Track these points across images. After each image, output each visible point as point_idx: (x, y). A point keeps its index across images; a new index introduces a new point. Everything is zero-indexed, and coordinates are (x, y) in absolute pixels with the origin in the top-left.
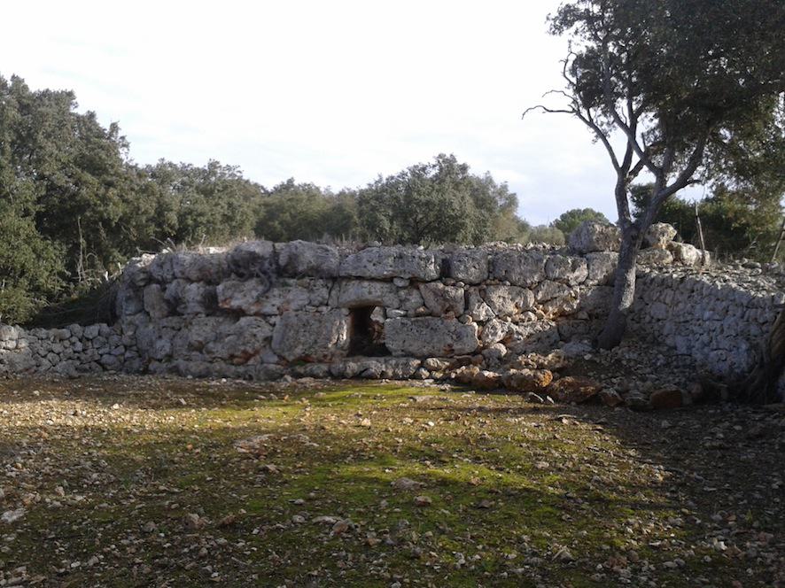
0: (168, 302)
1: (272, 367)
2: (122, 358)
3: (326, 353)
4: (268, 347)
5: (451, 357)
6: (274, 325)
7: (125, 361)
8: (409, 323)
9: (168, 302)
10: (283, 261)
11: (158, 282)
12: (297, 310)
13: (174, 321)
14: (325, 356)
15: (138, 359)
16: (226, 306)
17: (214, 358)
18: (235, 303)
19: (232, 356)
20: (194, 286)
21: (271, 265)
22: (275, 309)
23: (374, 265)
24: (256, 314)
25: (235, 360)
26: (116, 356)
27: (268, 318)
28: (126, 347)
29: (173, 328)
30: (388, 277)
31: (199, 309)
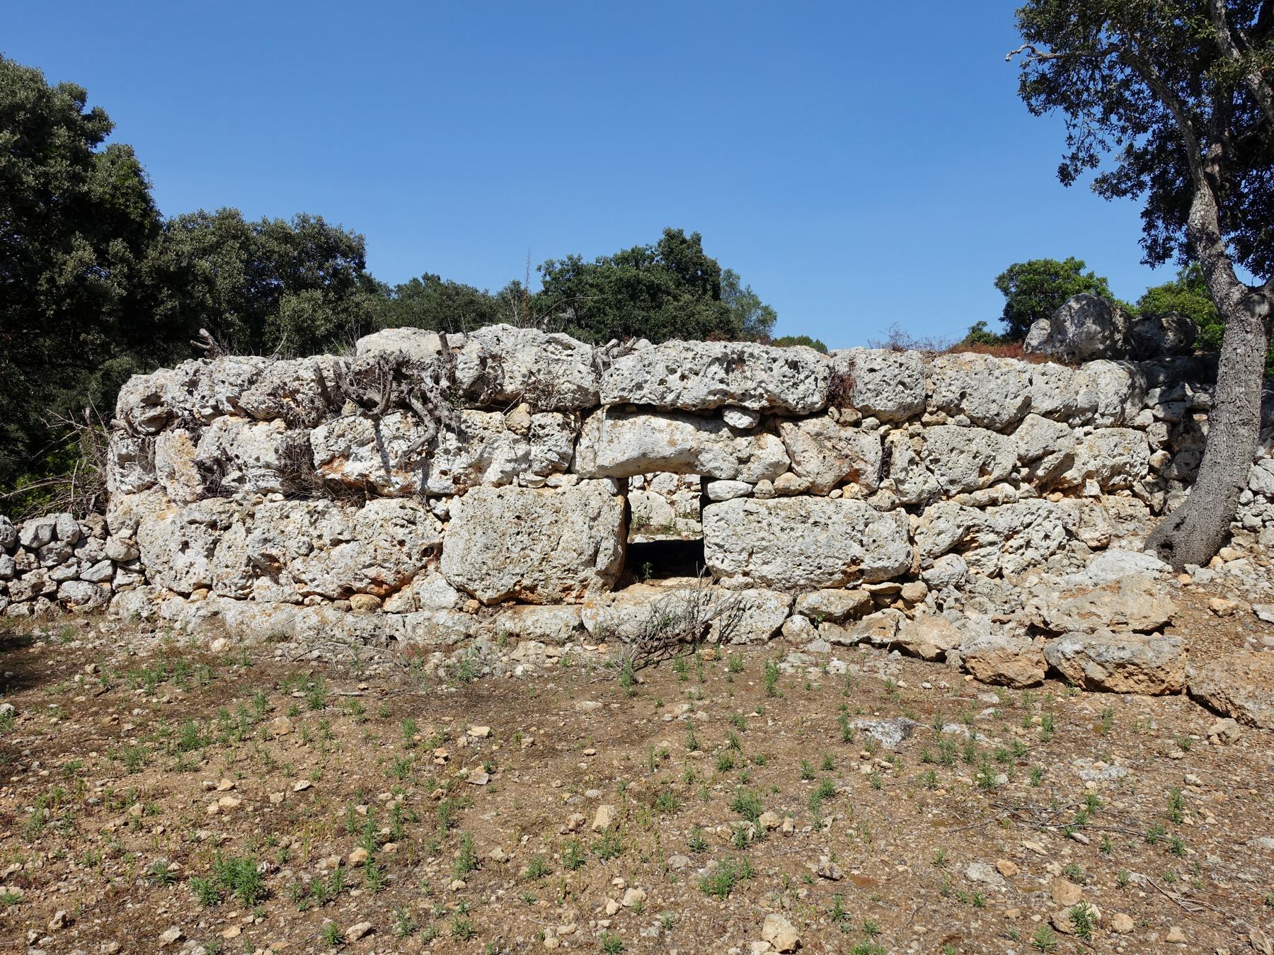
0: (201, 465)
1: (442, 617)
2: (107, 586)
3: (570, 582)
4: (431, 567)
5: (855, 588)
6: (446, 518)
7: (113, 593)
8: (764, 511)
9: (201, 465)
10: (466, 375)
11: (185, 424)
12: (499, 484)
13: (213, 505)
14: (568, 589)
15: (141, 590)
16: (337, 476)
17: (305, 595)
18: (351, 469)
19: (348, 592)
20: (262, 426)
21: (437, 380)
22: (447, 483)
23: (683, 377)
24: (406, 492)
25: (355, 600)
26: (91, 582)
27: (432, 501)
28: (115, 564)
29: (213, 525)
30: (712, 406)
31: (274, 483)
